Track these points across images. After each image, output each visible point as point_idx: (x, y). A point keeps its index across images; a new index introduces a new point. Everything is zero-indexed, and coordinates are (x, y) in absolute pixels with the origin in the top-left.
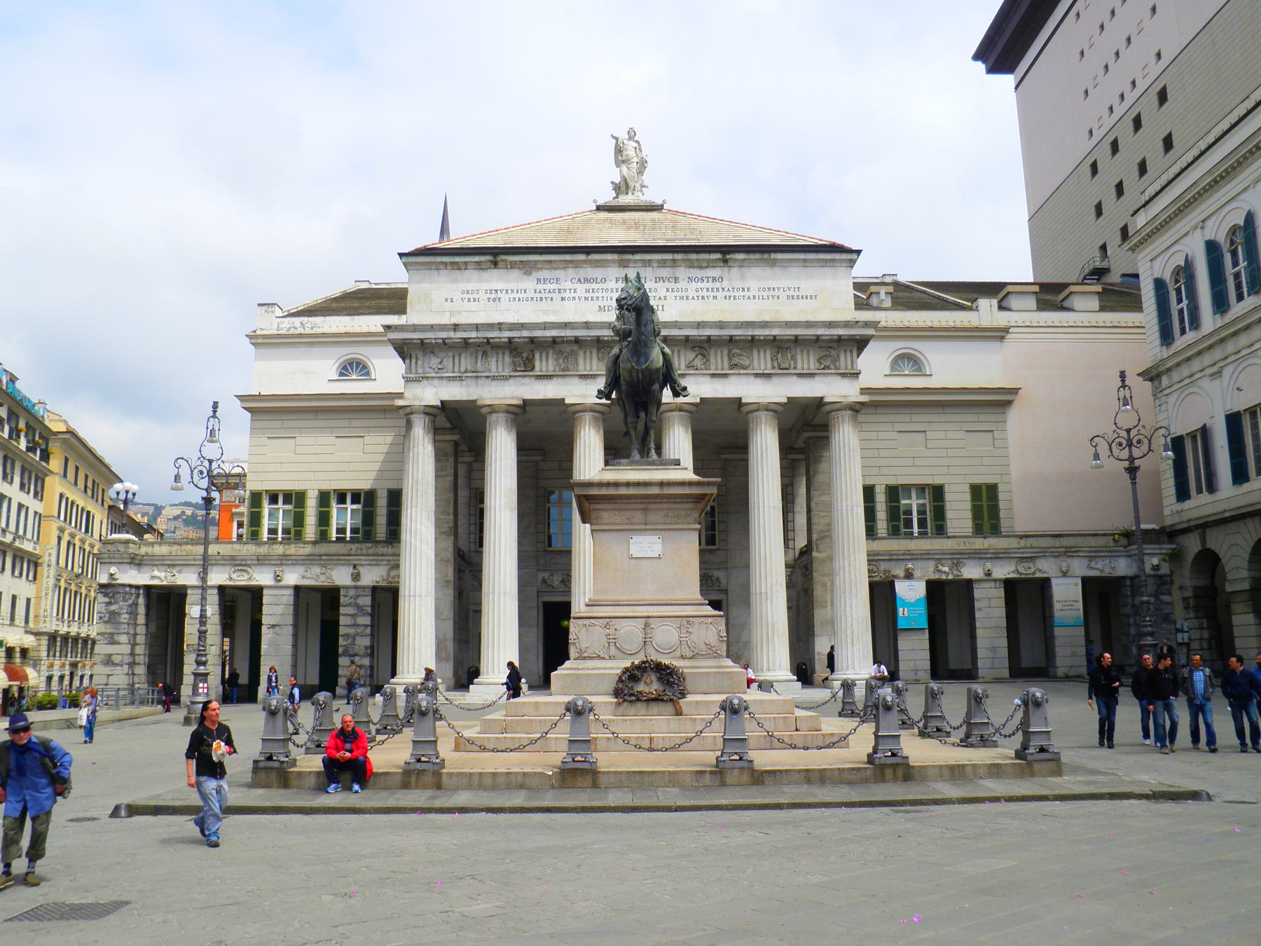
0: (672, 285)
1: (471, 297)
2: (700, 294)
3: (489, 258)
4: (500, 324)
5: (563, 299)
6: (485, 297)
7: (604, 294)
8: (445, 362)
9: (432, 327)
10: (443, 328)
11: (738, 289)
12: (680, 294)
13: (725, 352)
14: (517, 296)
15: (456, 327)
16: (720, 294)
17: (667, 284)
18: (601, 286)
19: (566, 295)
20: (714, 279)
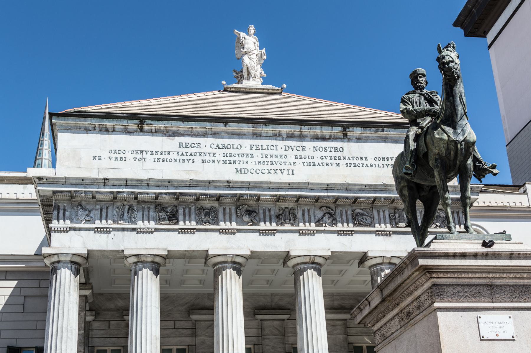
0: (300, 153)
1: (119, 156)
2: (324, 161)
3: (137, 122)
4: (148, 180)
5: (203, 161)
6: (128, 155)
7: (241, 159)
8: (91, 215)
9: (82, 182)
10: (94, 182)
11: (357, 158)
12: (309, 161)
13: (349, 212)
14: (162, 157)
15: (105, 182)
16: (342, 162)
17: (295, 152)
18: (237, 151)
19: (207, 158)
20: (336, 150)
